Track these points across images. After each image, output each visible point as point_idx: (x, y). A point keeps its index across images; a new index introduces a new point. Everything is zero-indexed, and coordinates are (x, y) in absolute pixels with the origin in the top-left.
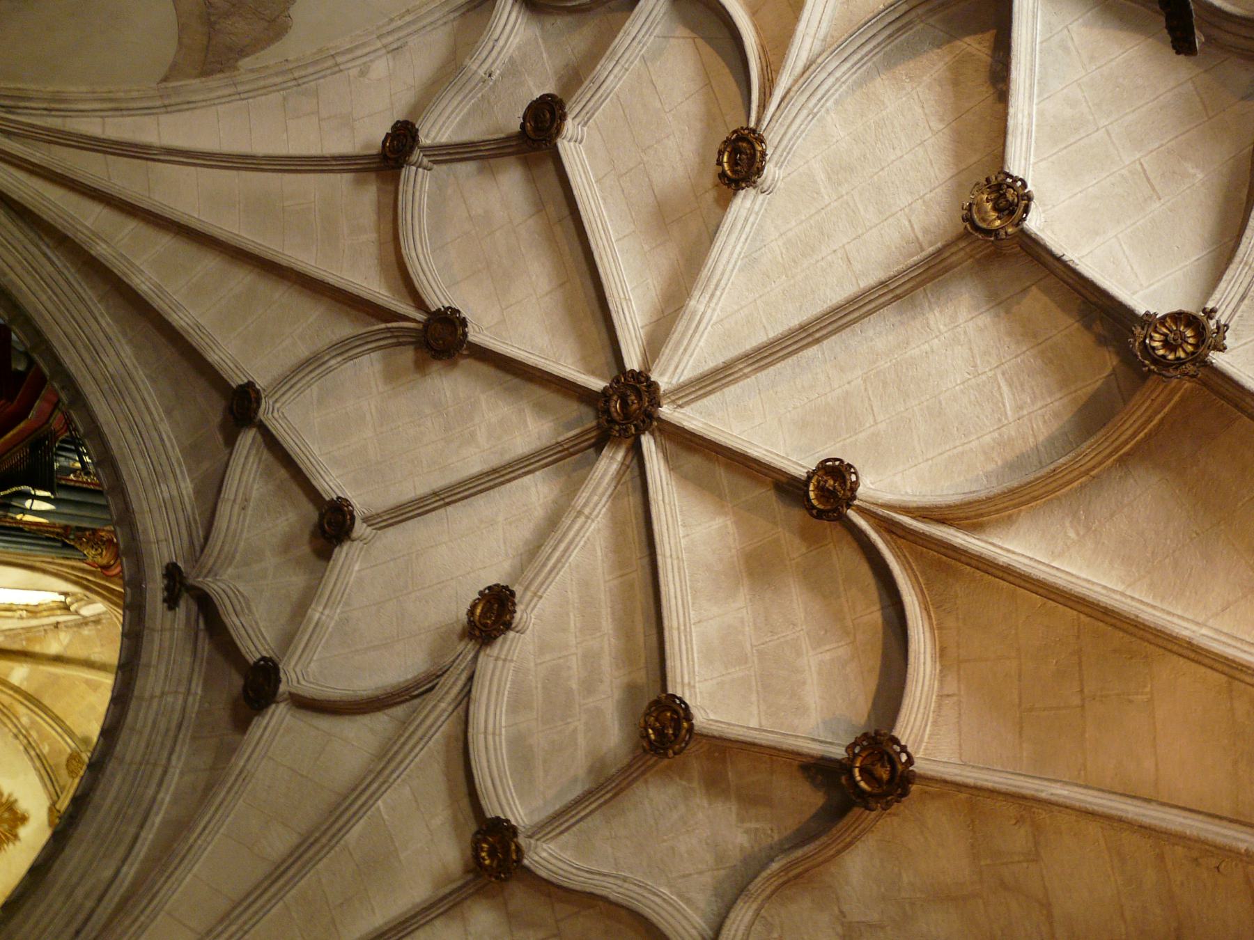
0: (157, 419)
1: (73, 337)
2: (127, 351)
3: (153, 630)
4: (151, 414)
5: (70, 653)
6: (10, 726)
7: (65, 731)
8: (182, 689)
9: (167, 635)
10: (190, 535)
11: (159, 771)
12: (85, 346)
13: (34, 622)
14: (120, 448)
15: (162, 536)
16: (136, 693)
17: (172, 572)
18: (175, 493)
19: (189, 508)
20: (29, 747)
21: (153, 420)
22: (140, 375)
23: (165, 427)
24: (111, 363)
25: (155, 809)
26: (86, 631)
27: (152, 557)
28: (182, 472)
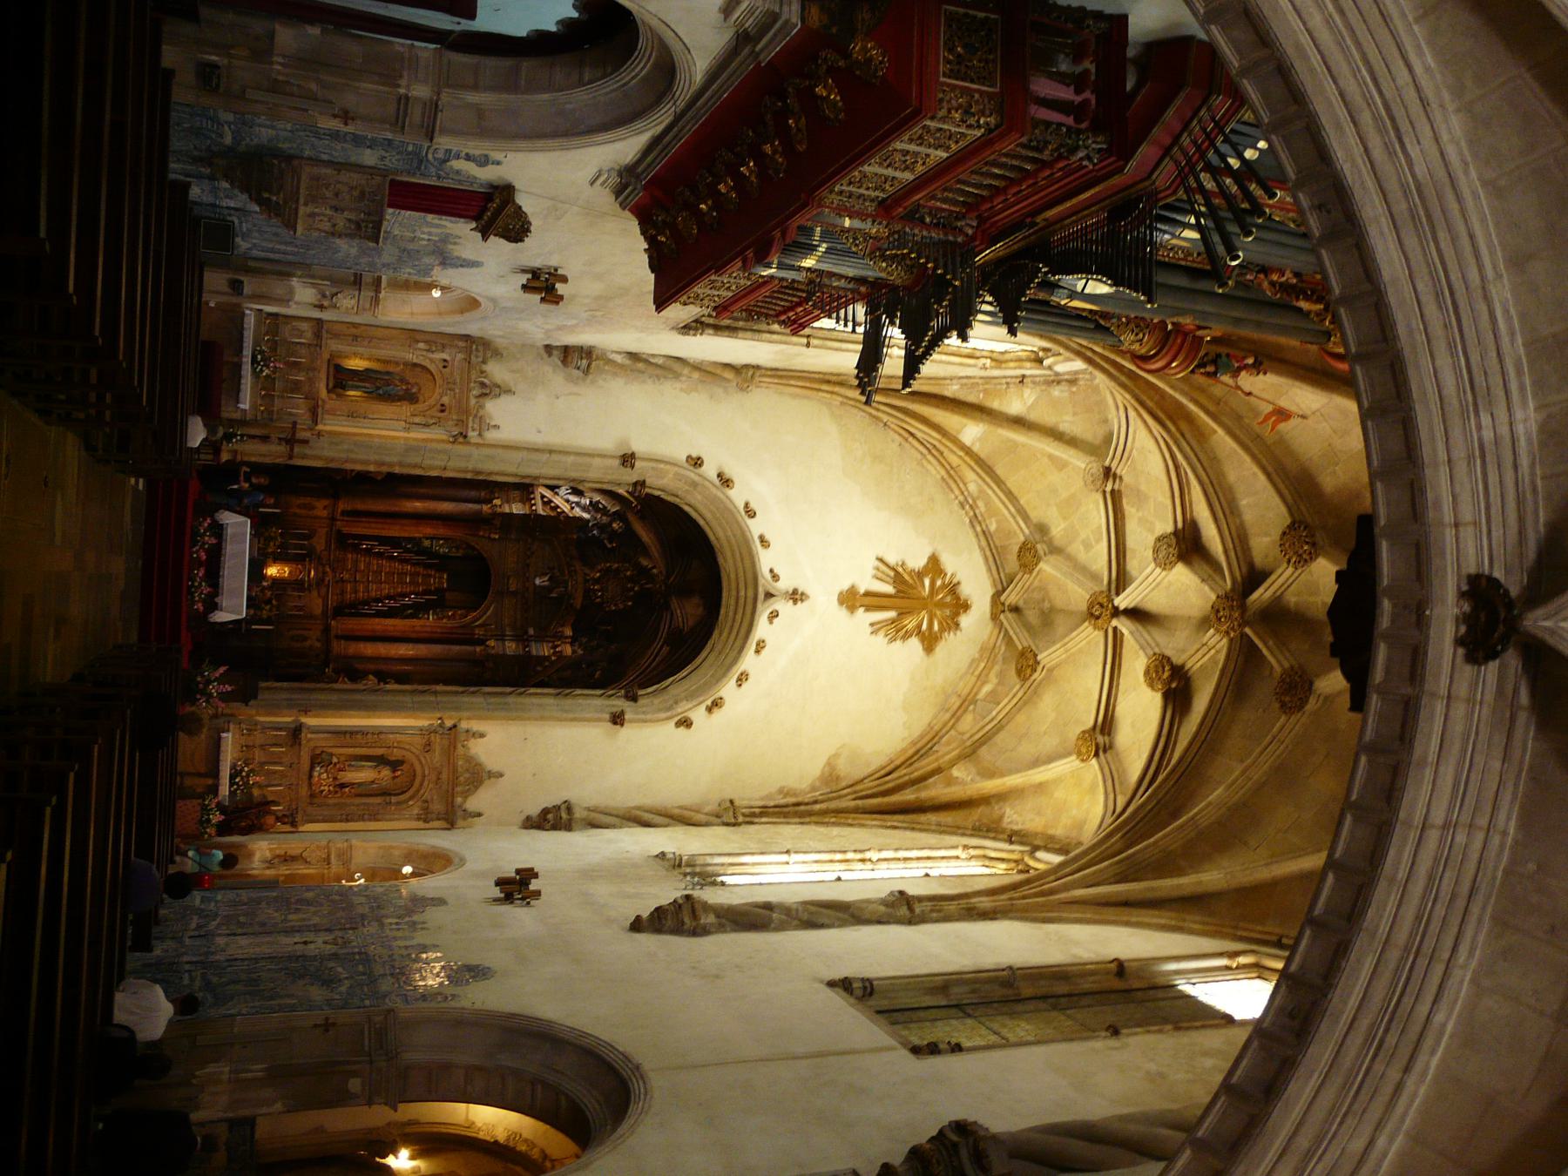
0: (1490, 273)
1: (1358, 100)
2: (1453, 127)
3: (1433, 695)
4: (1481, 267)
5: (1033, 416)
6: (957, 492)
7: (1018, 511)
8: (1483, 821)
9: (1459, 710)
10: (1521, 520)
11: (1439, 969)
12: (1376, 118)
13: (996, 373)
14: (1411, 332)
15: (1467, 515)
16: (1402, 815)
17: (1480, 590)
18: (1504, 430)
19: (1524, 462)
20: (975, 520)
21: (1483, 278)
22: (1470, 180)
23: (1502, 292)
24: (1421, 153)
25: (1428, 1042)
26: (1056, 392)
27: (1443, 553)
28: (1522, 388)
